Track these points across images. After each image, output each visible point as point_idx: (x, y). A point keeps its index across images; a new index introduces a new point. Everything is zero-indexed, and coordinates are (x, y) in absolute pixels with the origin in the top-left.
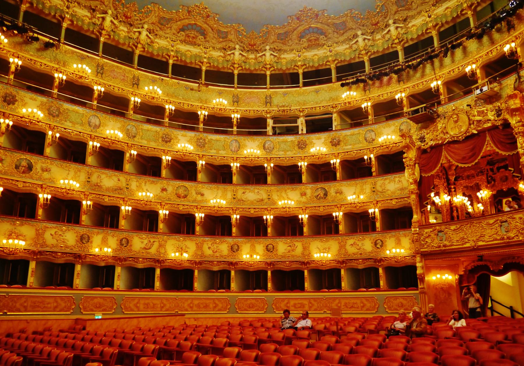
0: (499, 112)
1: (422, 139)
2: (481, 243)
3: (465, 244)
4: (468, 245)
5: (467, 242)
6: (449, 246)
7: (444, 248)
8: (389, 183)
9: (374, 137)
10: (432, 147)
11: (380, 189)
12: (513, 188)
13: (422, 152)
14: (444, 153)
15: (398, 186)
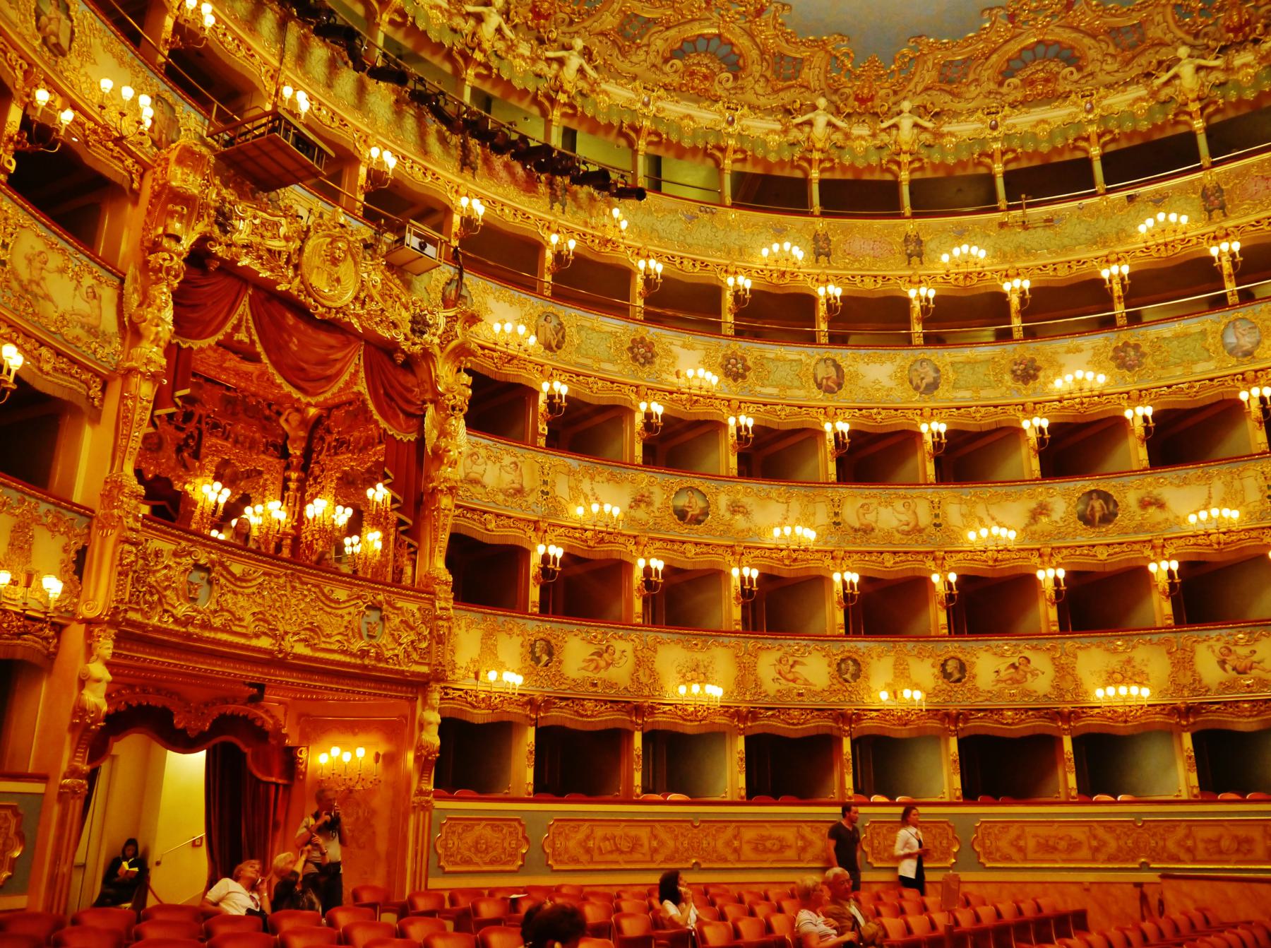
0: (419, 325)
1: (224, 220)
2: (301, 649)
3: (257, 636)
4: (265, 643)
5: (265, 634)
6: (216, 630)
7: (197, 631)
8: (63, 271)
9: (64, 43)
10: (229, 268)
11: (25, 275)
12: (169, 484)
13: (199, 256)
14: (244, 308)
15: (82, 306)
